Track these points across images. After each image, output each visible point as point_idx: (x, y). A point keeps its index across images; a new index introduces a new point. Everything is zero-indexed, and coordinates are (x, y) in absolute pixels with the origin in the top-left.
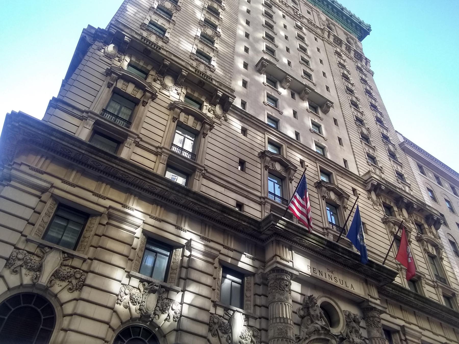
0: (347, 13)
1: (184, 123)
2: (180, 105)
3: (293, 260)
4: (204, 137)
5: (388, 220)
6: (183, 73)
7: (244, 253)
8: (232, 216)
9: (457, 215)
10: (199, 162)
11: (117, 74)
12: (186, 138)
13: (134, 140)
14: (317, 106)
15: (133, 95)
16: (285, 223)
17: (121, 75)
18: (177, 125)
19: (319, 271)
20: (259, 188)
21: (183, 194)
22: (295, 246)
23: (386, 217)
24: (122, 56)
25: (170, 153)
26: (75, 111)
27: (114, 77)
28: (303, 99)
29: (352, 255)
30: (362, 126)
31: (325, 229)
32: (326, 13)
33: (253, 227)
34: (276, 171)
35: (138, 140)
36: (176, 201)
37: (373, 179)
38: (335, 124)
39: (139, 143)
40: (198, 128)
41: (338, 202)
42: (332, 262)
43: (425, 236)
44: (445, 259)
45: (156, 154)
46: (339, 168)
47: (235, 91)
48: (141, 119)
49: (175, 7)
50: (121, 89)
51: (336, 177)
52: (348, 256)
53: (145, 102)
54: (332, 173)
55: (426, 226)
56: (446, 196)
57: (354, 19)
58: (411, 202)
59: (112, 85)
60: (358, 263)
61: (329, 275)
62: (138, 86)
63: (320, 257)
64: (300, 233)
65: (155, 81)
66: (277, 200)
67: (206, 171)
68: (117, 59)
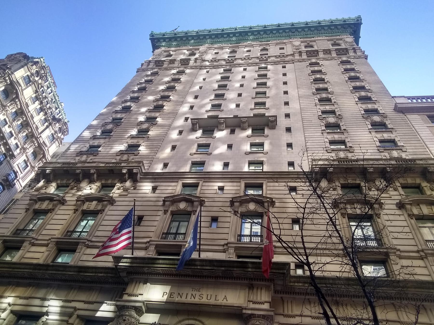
0: (327, 23)
7: (105, 302)
8: (89, 273)
14: (264, 126)
16: (130, 260)
21: (43, 270)
22: (151, 277)
28: (244, 129)
29: (215, 264)
32: (304, 37)
33: (110, 275)
35: (33, 241)
36: (44, 277)
41: (260, 210)
42: (200, 280)
45: (47, 245)
46: (269, 175)
52: (210, 266)
57: (336, 23)
60: (225, 270)
61: (192, 294)
63: (181, 278)
64: (146, 264)
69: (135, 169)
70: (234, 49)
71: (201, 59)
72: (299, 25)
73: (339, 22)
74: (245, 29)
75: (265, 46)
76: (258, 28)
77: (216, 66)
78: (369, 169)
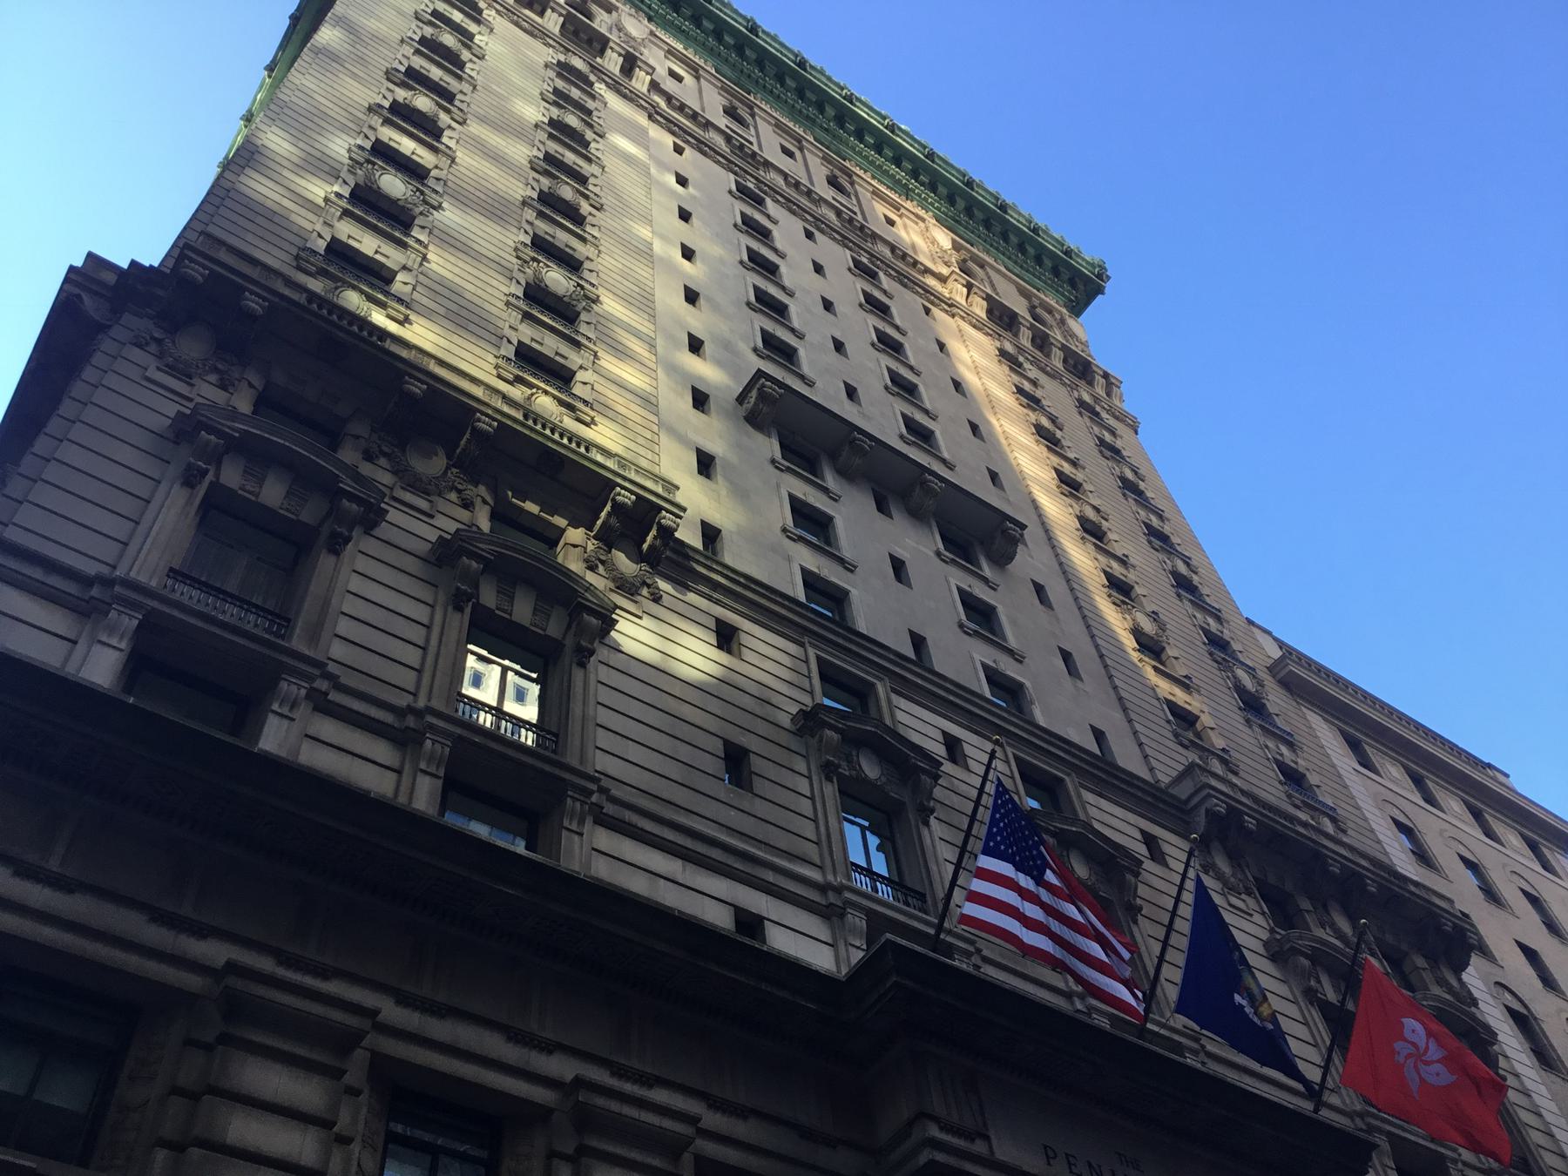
1: (497, 612)
2: (481, 545)
3: (985, 1124)
4: (582, 665)
5: (1288, 946)
6: (481, 424)
9: (1513, 914)
10: (575, 763)
11: (219, 434)
12: (510, 675)
13: (306, 685)
15: (287, 510)
17: (237, 435)
18: (473, 624)
19: (1090, 1165)
20: (812, 851)
23: (1278, 937)
24: (233, 368)
25: (459, 731)
26: (55, 581)
27: (208, 442)
30: (1134, 607)
31: (1076, 999)
34: (866, 781)
35: (322, 685)
37: (1211, 792)
38: (1041, 602)
39: (329, 697)
40: (554, 629)
43: (1425, 999)
44: (1511, 1081)
47: (678, 488)
48: (326, 603)
49: (418, 193)
50: (240, 492)
51: (1079, 796)
53: (341, 534)
54: (1062, 780)
55: (1420, 962)
56: (1460, 846)
58: (1354, 874)
59: (205, 473)
62: (305, 479)
65: (369, 457)
66: (884, 891)
67: (604, 797)
68: (213, 378)
69: (668, 511)
70: (737, 104)
71: (651, 71)
72: (947, 171)
73: (1053, 245)
74: (781, 53)
75: (838, 173)
76: (826, 85)
77: (706, 145)
78: (1331, 865)
